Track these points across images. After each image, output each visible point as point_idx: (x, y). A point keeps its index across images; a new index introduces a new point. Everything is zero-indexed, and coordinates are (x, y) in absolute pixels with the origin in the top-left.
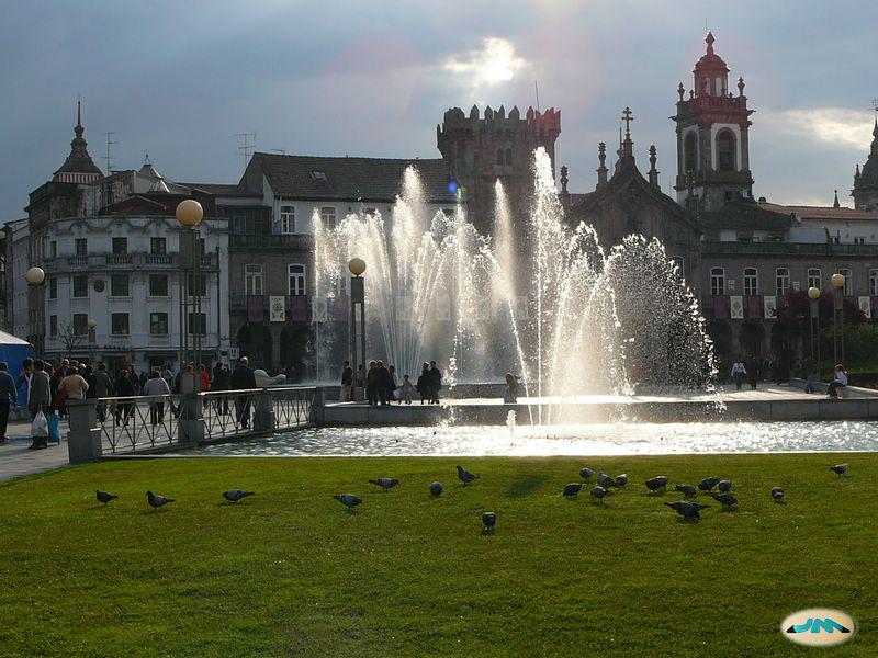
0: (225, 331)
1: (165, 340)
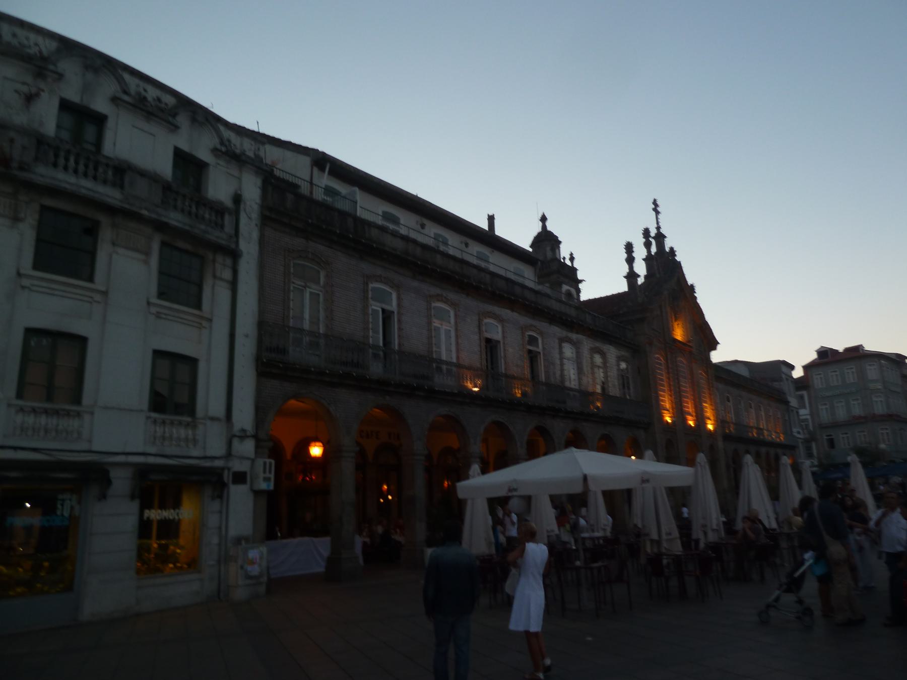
0: (244, 417)
1: (74, 423)
